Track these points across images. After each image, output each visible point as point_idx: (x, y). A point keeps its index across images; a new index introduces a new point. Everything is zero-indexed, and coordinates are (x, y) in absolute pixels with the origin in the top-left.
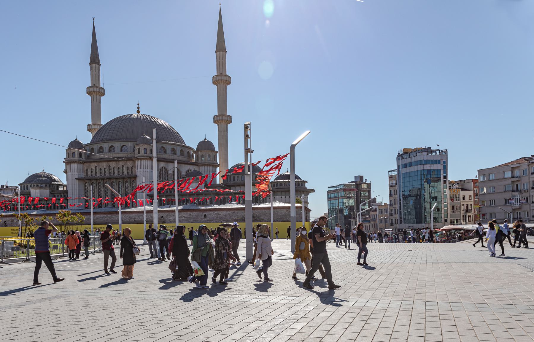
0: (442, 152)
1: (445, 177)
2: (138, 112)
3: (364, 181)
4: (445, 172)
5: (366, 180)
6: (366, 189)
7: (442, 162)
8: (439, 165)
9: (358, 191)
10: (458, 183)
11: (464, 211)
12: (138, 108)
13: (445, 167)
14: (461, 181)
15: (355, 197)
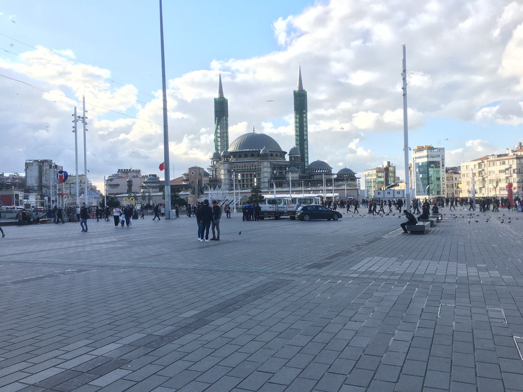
0: (441, 149)
1: (443, 165)
2: (254, 131)
3: (391, 165)
4: (443, 162)
5: (392, 164)
6: (392, 171)
7: (441, 156)
8: (439, 158)
9: (386, 172)
10: (452, 169)
11: (456, 188)
12: (254, 128)
13: (443, 159)
14: (455, 167)
15: (385, 177)
